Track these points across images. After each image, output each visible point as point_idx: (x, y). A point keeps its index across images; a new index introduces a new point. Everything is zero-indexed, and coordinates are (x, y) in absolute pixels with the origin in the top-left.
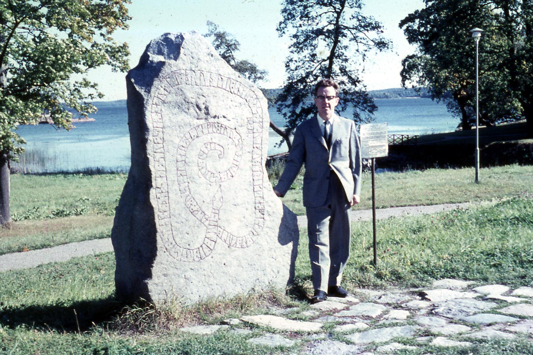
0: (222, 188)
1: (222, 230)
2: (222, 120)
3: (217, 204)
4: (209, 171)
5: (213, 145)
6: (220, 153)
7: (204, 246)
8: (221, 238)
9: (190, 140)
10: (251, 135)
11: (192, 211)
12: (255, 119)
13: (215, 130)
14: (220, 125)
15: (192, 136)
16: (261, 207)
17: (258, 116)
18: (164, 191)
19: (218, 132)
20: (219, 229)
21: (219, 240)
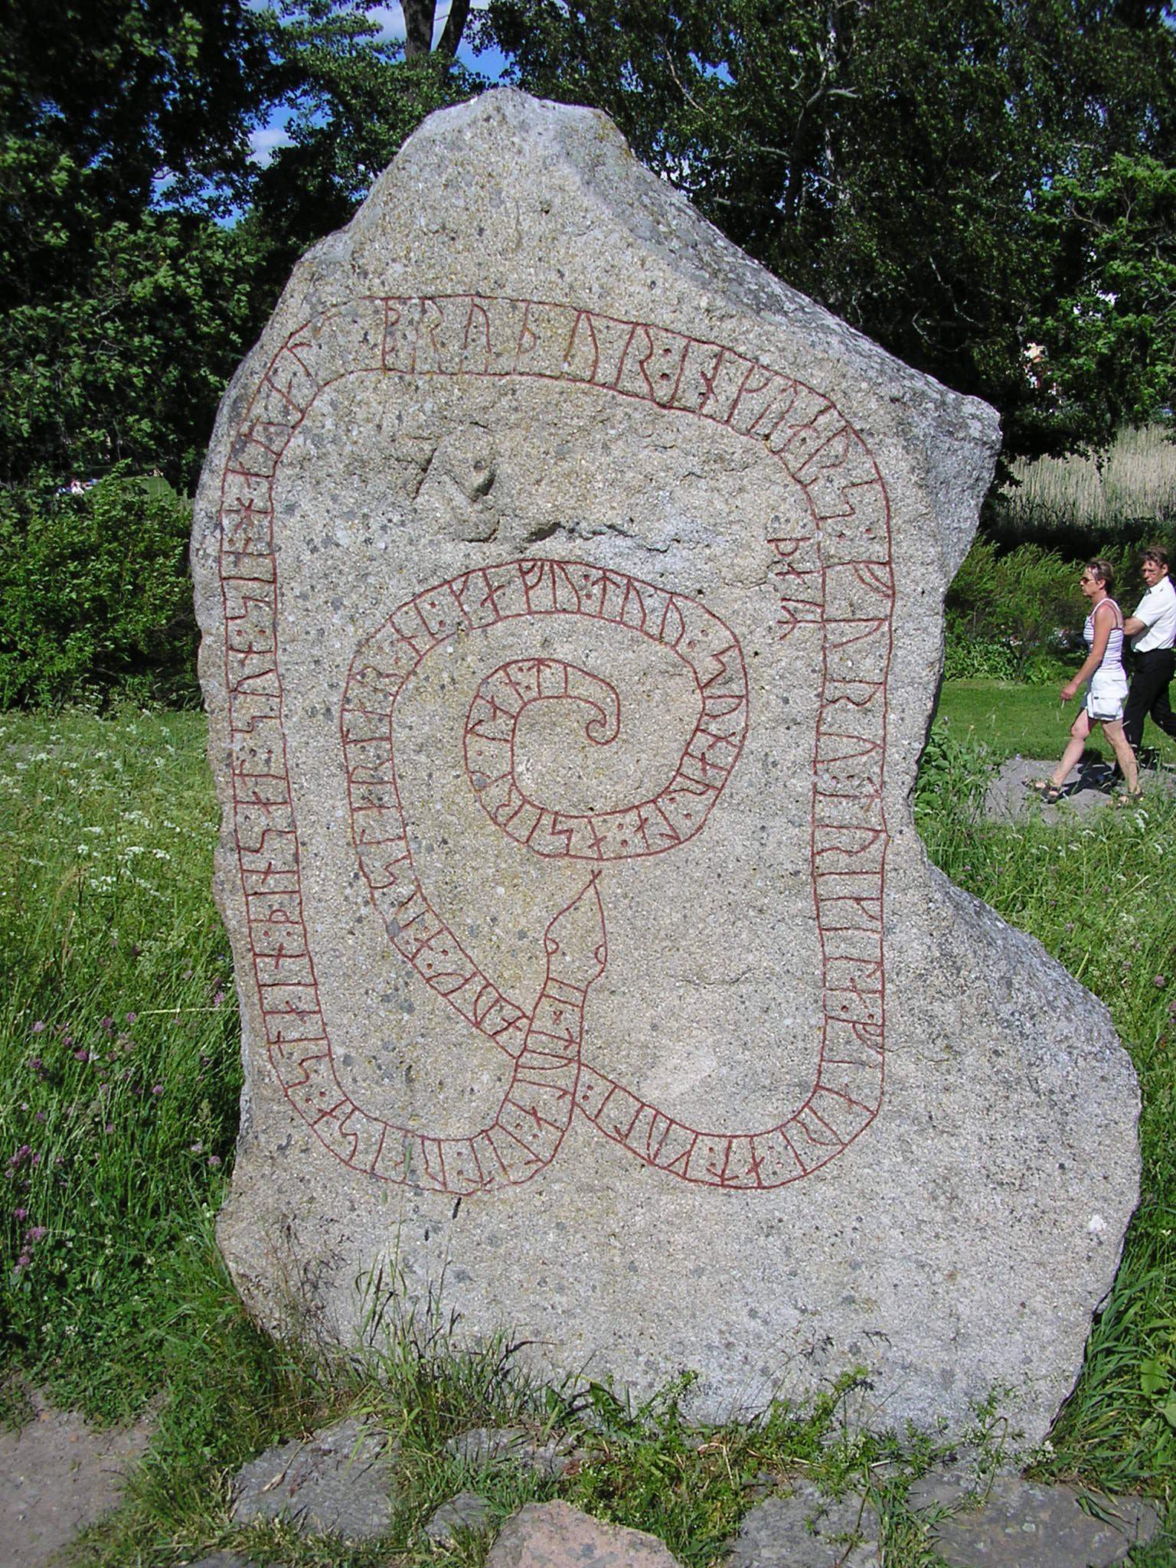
0: (608, 886)
2: (606, 550)
3: (572, 963)
4: (525, 801)
7: (496, 1135)
9: (423, 643)
13: (563, 594)
14: (596, 574)
15: (434, 626)
16: (858, 1011)
18: (277, 864)
20: (586, 1076)
21: (582, 1128)
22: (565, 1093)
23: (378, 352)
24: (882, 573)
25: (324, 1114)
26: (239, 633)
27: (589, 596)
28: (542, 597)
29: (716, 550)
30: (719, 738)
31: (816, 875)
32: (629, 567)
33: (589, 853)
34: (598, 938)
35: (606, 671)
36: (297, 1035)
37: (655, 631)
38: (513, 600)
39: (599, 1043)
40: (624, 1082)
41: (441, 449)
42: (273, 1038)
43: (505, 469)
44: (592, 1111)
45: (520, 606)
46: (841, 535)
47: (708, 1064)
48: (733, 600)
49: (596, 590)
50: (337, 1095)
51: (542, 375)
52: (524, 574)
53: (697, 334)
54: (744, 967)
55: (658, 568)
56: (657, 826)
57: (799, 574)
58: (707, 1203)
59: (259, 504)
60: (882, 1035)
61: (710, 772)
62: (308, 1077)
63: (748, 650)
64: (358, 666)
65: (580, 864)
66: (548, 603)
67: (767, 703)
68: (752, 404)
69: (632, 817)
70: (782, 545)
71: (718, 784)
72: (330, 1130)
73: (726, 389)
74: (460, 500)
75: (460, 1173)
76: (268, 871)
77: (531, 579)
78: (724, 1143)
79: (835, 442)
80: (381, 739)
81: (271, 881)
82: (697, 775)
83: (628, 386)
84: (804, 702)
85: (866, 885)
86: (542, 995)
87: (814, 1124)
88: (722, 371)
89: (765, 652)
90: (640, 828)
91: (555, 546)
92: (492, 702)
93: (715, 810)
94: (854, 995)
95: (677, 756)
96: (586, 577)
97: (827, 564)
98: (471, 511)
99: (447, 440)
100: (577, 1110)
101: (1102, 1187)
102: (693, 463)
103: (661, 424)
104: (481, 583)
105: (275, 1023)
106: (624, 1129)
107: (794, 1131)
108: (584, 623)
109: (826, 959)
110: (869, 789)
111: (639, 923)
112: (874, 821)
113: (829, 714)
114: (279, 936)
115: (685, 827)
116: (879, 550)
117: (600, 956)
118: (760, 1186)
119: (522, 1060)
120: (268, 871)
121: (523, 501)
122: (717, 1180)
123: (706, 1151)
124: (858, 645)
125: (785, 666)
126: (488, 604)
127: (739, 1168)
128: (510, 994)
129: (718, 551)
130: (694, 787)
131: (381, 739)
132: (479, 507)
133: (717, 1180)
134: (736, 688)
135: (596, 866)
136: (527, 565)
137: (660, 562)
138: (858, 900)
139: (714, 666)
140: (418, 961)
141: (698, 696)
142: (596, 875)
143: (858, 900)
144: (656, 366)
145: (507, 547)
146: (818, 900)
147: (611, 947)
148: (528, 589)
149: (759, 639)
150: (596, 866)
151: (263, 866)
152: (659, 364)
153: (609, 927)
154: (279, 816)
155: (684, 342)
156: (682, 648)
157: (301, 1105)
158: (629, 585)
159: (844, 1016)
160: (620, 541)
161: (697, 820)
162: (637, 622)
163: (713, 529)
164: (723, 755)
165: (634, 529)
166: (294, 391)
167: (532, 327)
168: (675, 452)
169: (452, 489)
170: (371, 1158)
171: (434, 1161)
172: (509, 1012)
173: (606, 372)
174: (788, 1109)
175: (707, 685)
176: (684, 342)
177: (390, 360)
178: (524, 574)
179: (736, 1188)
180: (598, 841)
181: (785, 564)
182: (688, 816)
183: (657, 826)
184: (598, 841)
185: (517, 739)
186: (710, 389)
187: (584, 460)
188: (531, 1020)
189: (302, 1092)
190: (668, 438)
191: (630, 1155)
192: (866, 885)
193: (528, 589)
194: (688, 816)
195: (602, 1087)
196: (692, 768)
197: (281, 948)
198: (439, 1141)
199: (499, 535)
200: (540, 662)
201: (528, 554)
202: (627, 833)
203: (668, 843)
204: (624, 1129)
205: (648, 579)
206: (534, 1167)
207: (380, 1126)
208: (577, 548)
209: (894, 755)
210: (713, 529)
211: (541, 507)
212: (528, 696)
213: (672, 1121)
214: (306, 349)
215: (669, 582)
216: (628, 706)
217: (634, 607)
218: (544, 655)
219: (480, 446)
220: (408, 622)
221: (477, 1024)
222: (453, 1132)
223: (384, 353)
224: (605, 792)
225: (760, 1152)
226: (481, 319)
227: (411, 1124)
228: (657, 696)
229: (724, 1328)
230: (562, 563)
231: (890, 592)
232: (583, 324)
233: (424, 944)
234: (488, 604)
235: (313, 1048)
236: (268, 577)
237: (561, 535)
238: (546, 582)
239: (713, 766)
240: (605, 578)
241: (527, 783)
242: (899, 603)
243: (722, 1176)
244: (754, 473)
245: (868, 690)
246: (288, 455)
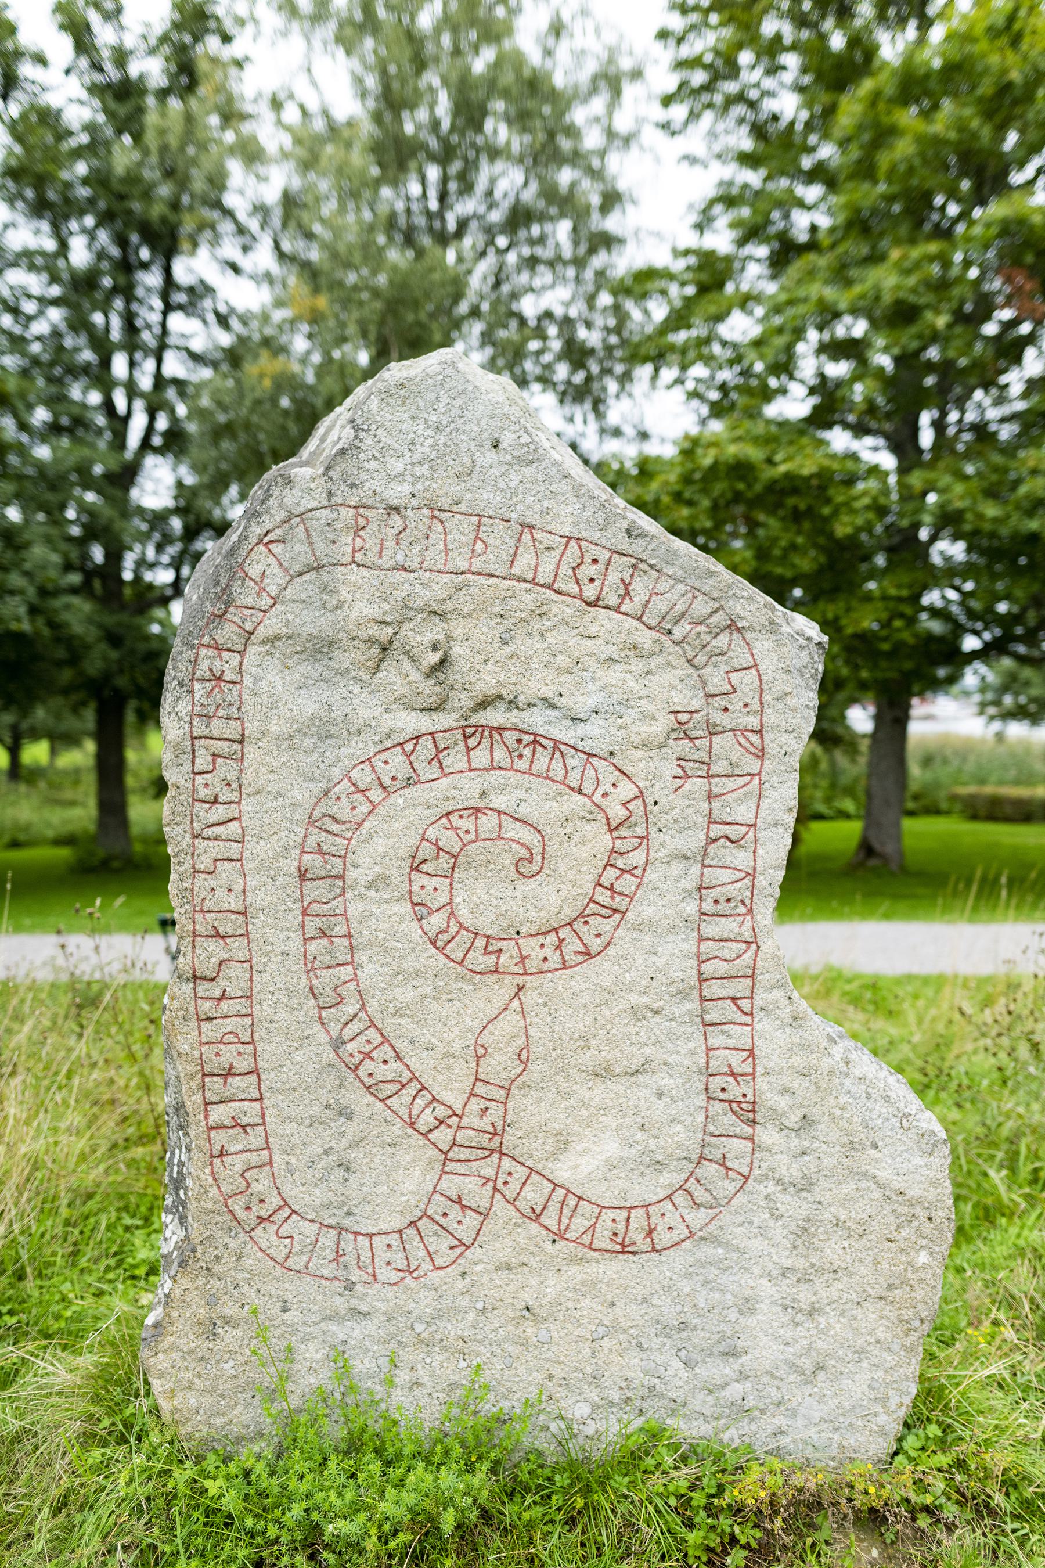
0: (530, 998)
1: (520, 1172)
2: (537, 720)
4: (461, 926)
5: (487, 823)
6: (524, 852)
8: (512, 1202)
9: (376, 795)
10: (696, 785)
11: (369, 1081)
12: (718, 717)
13: (500, 754)
14: (528, 738)
15: (387, 781)
16: (735, 1091)
17: (736, 705)
19: (522, 765)
22: (488, 1180)
23: (349, 549)
24: (754, 738)
25: (261, 1219)
26: (206, 785)
27: (521, 756)
28: (481, 757)
29: (627, 720)
30: (624, 871)
31: (702, 980)
32: (556, 733)
33: (516, 970)
34: (521, 1041)
35: (534, 818)
36: (239, 1147)
37: (575, 784)
38: (455, 760)
39: (519, 1133)
40: (539, 1167)
41: (403, 633)
42: (216, 1152)
43: (458, 650)
44: (510, 1194)
45: (463, 765)
46: (726, 709)
47: (611, 1147)
48: (638, 763)
49: (527, 752)
50: (277, 1201)
51: (491, 575)
52: (466, 737)
53: (620, 547)
54: (642, 1060)
55: (580, 733)
56: (573, 945)
57: (692, 739)
58: (611, 1269)
59: (229, 676)
60: (753, 1111)
61: (618, 899)
62: (249, 1185)
63: (650, 801)
64: (317, 814)
65: (508, 979)
66: (486, 762)
67: (666, 843)
68: (659, 605)
69: (552, 938)
70: (680, 716)
71: (623, 909)
72: (266, 1236)
74: (415, 676)
75: (389, 1263)
76: (223, 997)
77: (472, 742)
78: (625, 1214)
79: (721, 637)
80: (336, 877)
81: (225, 1005)
82: (607, 902)
83: (563, 588)
84: (694, 841)
85: (740, 987)
86: (472, 1094)
87: (699, 1193)
88: (637, 579)
89: (662, 801)
90: (559, 947)
91: (495, 716)
92: (436, 844)
93: (620, 930)
94: (731, 1079)
95: (591, 886)
96: (519, 741)
97: (713, 730)
98: (428, 688)
99: (407, 626)
100: (498, 1196)
101: (927, 1228)
102: (612, 651)
103: (587, 618)
104: (430, 745)
105: (219, 1138)
106: (538, 1210)
107: (679, 1198)
108: (515, 778)
109: (708, 1049)
110: (742, 910)
111: (558, 1028)
112: (747, 935)
113: (712, 850)
114: (228, 1055)
115: (595, 945)
116: (754, 722)
117: (523, 1058)
118: (654, 1250)
119: (450, 1155)
120: (223, 997)
121: (472, 678)
122: (618, 1248)
123: (609, 1223)
124: (735, 795)
125: (680, 812)
126: (435, 762)
127: (637, 1236)
128: (445, 1096)
129: (629, 721)
130: (602, 911)
131: (336, 877)
132: (432, 682)
133: (618, 1248)
134: (640, 831)
135: (520, 980)
136: (471, 730)
137: (581, 730)
138: (734, 999)
139: (623, 813)
140: (360, 1072)
141: (608, 837)
142: (520, 988)
143: (734, 999)
144: (588, 570)
145: (454, 716)
146: (703, 999)
147: (533, 1048)
148: (469, 750)
149: (659, 791)
150: (520, 980)
151: (218, 993)
152: (588, 570)
153: (531, 1032)
154: (237, 948)
155: (608, 555)
156: (597, 798)
157: (241, 1214)
158: (555, 747)
159: (723, 1096)
160: (549, 712)
161: (605, 939)
162: (560, 778)
163: (626, 703)
164: (626, 885)
165: (562, 702)
166: (266, 581)
167: (482, 535)
168: (598, 641)
169: (407, 666)
170: (305, 1258)
171: (365, 1254)
172: (441, 1112)
173: (545, 574)
174: (677, 1179)
175: (617, 828)
176: (608, 555)
177: (359, 557)
178: (466, 737)
179: (634, 1253)
180: (523, 959)
181: (681, 731)
182: (598, 935)
183: (573, 945)
184: (523, 959)
185: (456, 875)
186: (627, 593)
187: (522, 645)
189: (242, 1200)
190: (593, 629)
191: (544, 1232)
192: (740, 987)
193: (469, 750)
194: (598, 935)
195: (520, 1172)
196: (603, 896)
197: (231, 1067)
198: (371, 1236)
199: (449, 706)
200: (478, 810)
201: (471, 722)
202: (548, 952)
203: (580, 958)
204: (538, 1210)
205: (571, 742)
207: (315, 1227)
208: (513, 718)
209: (761, 881)
210: (626, 703)
211: (487, 682)
212: (466, 838)
213: (580, 1198)
214: (281, 546)
215: (586, 745)
216: (552, 847)
217: (557, 764)
218: (481, 805)
219: (435, 632)
220: (363, 776)
221: (412, 1125)
222: (384, 1227)
223: (354, 551)
224: (534, 917)
225: (653, 1221)
226: (440, 528)
227: (345, 1222)
228: (576, 838)
229: (623, 1384)
230: (500, 729)
232: (526, 537)
233: (368, 1055)
234: (435, 762)
235: (254, 1158)
236: (238, 737)
237: (502, 706)
238: (485, 744)
239: (620, 894)
240: (535, 742)
241: (464, 913)
242: (767, 762)
243: (622, 1244)
244: (659, 660)
245: (745, 829)
246: (261, 632)
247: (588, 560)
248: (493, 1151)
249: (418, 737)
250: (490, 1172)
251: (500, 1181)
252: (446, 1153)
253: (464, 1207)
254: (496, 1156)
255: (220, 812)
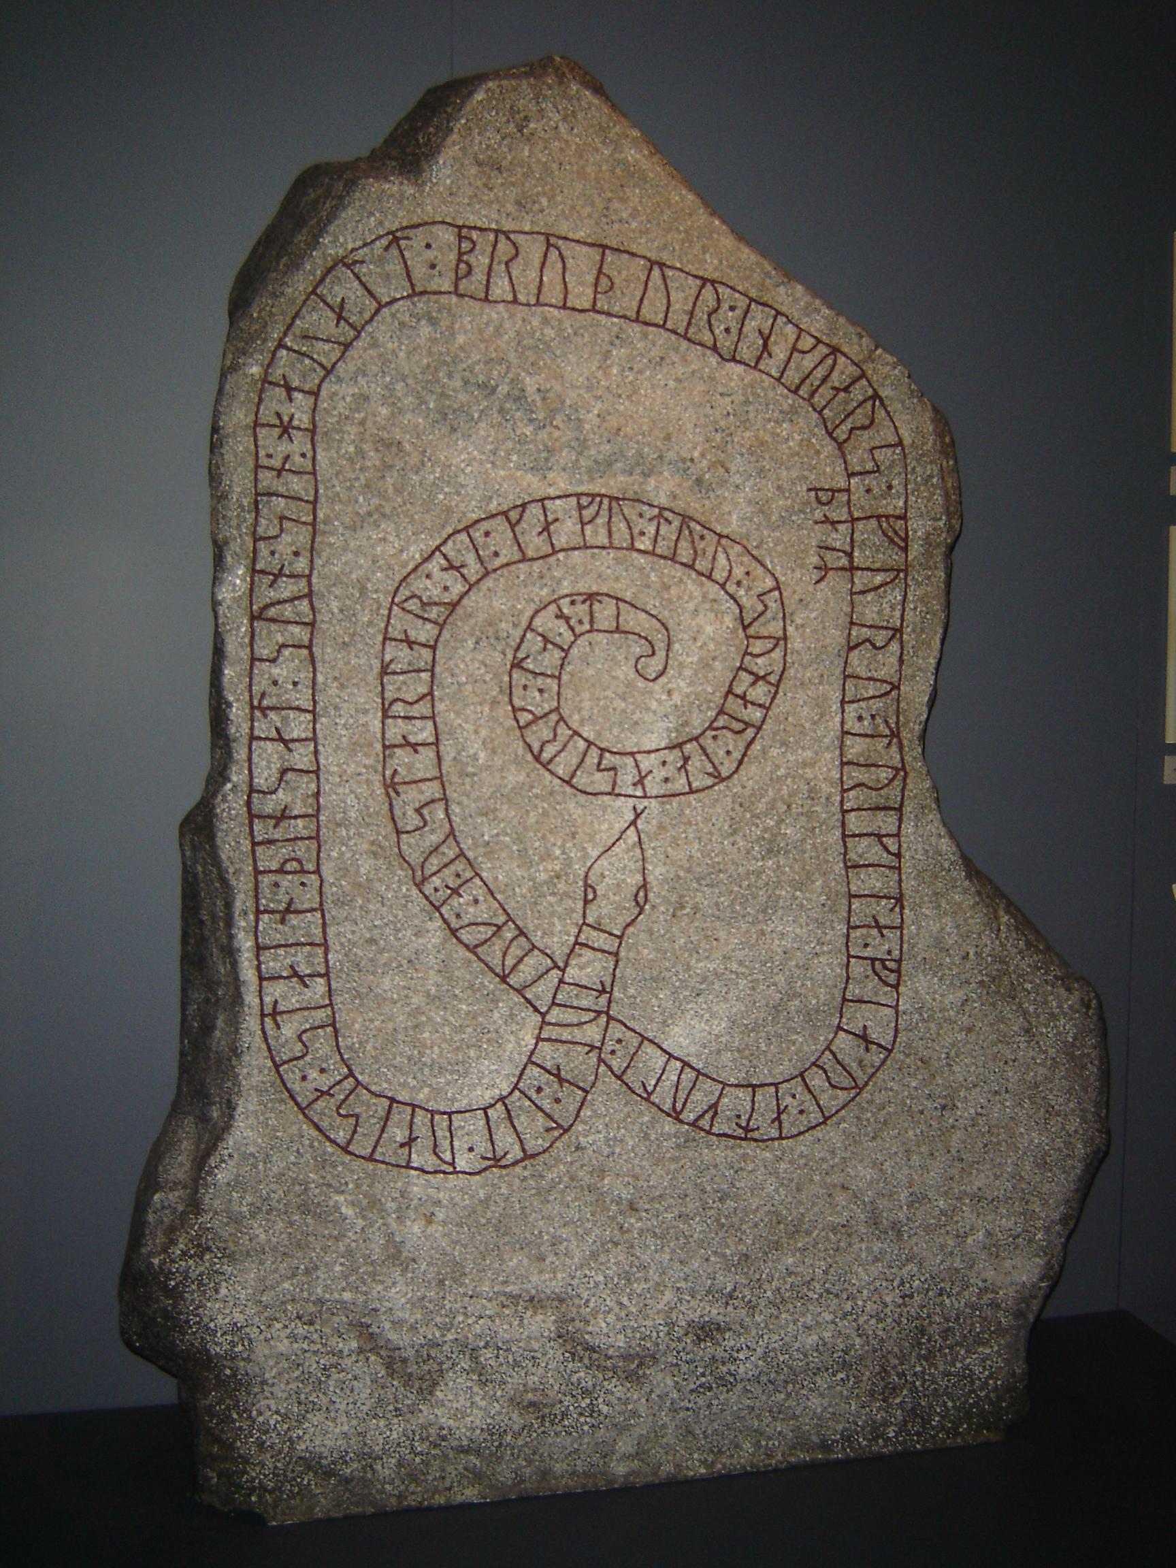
20: (616, 1031)
22: (593, 1047)
42: (268, 1009)
52: (580, 508)
73: (780, 352)
77: (588, 514)
105: (275, 991)
119: (548, 1018)
122: (740, 1132)
134: (775, 628)
138: (879, 837)
188: (563, 971)
206: (556, 1134)
231: (903, 544)
240: (660, 515)
243: (747, 1129)
247: (725, 306)
248: (599, 1013)
249: (524, 506)
250: (596, 1039)
251: (608, 1047)
252: (543, 1015)
253: (561, 1081)
254: (604, 1018)
255: (287, 588)
